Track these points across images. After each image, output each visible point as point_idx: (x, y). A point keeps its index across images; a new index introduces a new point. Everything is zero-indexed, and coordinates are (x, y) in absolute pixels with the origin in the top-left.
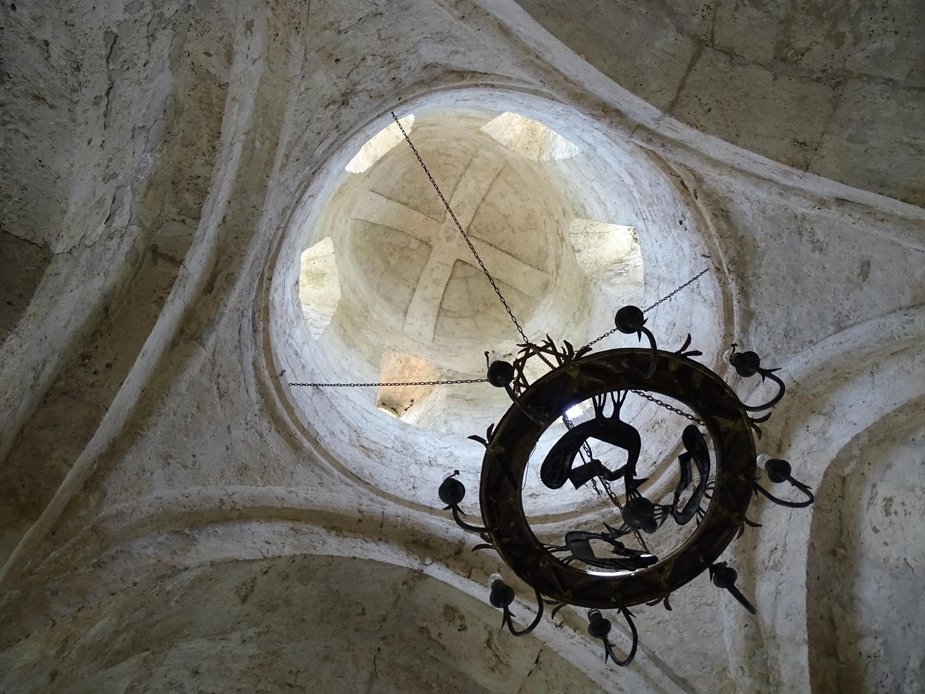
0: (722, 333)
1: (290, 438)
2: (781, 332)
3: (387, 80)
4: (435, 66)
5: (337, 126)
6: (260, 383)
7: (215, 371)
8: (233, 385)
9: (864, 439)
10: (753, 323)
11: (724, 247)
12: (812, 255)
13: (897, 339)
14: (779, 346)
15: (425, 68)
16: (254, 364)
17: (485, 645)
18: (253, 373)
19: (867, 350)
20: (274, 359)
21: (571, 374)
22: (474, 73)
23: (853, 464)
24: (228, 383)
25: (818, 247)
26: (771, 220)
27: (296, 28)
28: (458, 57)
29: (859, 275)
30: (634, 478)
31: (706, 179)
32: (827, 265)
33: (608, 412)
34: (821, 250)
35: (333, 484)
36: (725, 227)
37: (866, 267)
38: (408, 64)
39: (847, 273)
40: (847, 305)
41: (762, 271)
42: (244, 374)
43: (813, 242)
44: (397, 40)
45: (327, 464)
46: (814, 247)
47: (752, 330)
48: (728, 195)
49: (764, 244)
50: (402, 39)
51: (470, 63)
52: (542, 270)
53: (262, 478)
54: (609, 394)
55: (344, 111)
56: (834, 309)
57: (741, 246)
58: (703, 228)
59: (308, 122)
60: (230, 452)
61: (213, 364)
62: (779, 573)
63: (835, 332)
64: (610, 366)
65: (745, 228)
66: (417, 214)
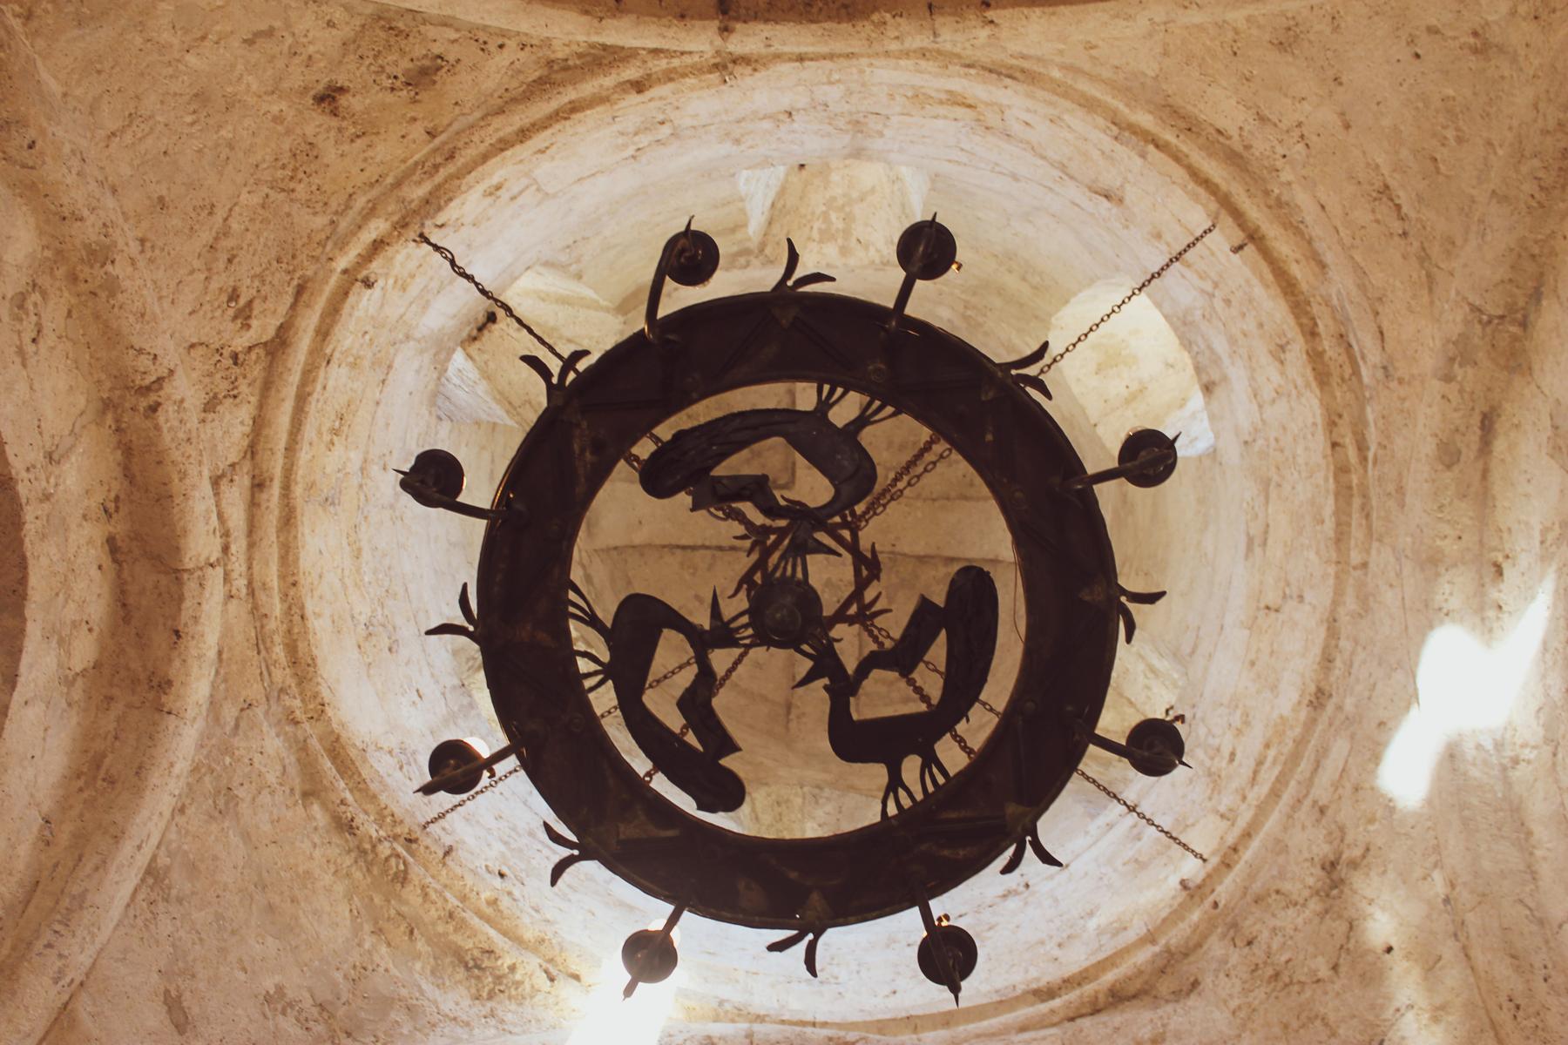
0: (330, 712)
1: (1190, 127)
2: (241, 792)
4: (1179, 995)
5: (1322, 811)
6: (1295, 228)
7: (1416, 244)
8: (1362, 215)
12: (277, 978)
13: (57, 927)
14: (228, 760)
15: (1195, 984)
16: (1323, 266)
18: (1320, 246)
20: (1270, 277)
21: (1021, 809)
22: (1096, 1011)
24: (1377, 221)
26: (387, 1002)
27: (1518, 1007)
29: (180, 997)
30: (826, 681)
32: (241, 976)
33: (911, 767)
34: (268, 999)
35: (1061, 52)
36: (458, 939)
38: (1238, 982)
39: (202, 986)
40: (165, 926)
41: (340, 888)
42: (1340, 241)
43: (290, 1005)
44: (1286, 1026)
45: (1083, 86)
46: (284, 995)
47: (291, 759)
48: (489, 1004)
49: (367, 946)
50: (1277, 1030)
51: (1117, 1029)
52: (608, 550)
53: (1236, 32)
54: (919, 796)
55: (1324, 850)
56: (180, 901)
60: (1331, 73)
61: (1424, 258)
62: (9, 296)
63: (154, 858)
64: (946, 853)
66: (920, 549)
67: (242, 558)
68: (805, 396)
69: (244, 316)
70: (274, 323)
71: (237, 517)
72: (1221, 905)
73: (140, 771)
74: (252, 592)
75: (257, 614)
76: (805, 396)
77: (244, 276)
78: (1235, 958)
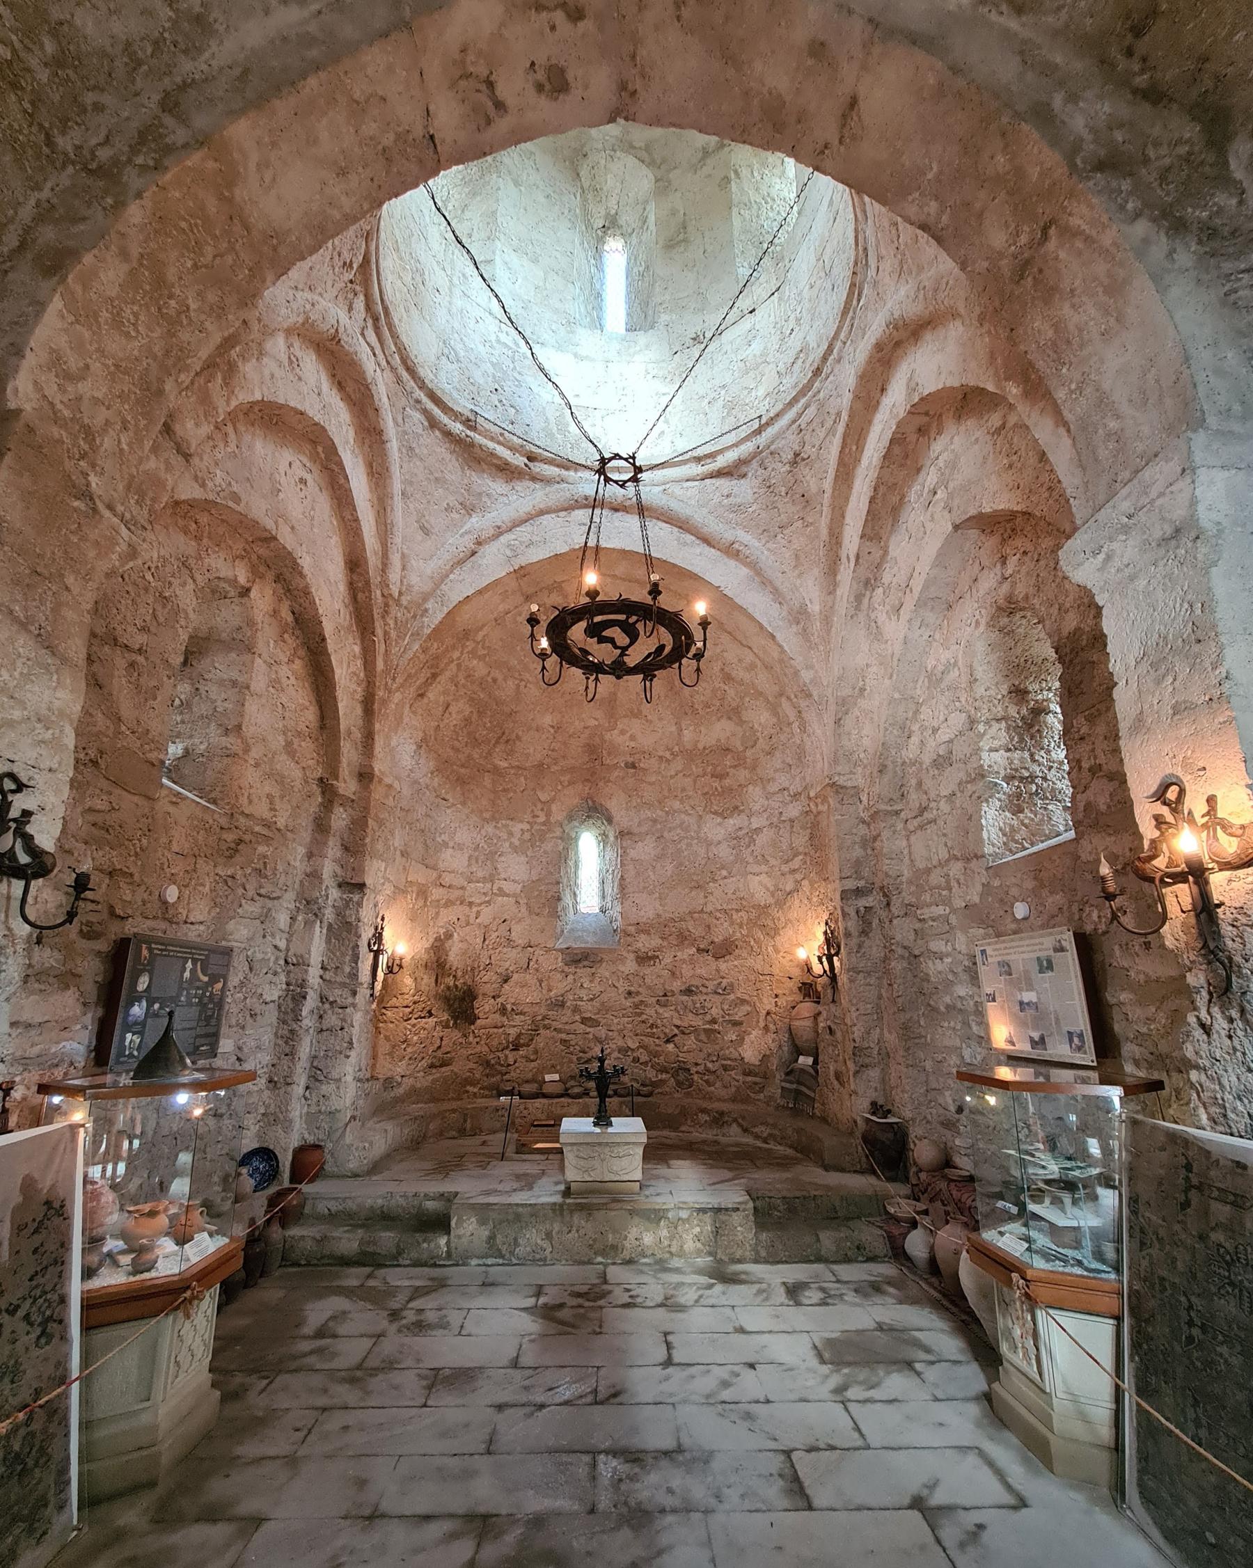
9: (342, 481)
10: (426, 424)
17: (492, 78)
23: (323, 456)
25: (449, 509)
26: (480, 494)
37: (426, 531)
47: (422, 418)
65: (483, 471)
69: (351, 265)
70: (361, 258)
74: (388, 362)
75: (393, 370)
77: (347, 256)
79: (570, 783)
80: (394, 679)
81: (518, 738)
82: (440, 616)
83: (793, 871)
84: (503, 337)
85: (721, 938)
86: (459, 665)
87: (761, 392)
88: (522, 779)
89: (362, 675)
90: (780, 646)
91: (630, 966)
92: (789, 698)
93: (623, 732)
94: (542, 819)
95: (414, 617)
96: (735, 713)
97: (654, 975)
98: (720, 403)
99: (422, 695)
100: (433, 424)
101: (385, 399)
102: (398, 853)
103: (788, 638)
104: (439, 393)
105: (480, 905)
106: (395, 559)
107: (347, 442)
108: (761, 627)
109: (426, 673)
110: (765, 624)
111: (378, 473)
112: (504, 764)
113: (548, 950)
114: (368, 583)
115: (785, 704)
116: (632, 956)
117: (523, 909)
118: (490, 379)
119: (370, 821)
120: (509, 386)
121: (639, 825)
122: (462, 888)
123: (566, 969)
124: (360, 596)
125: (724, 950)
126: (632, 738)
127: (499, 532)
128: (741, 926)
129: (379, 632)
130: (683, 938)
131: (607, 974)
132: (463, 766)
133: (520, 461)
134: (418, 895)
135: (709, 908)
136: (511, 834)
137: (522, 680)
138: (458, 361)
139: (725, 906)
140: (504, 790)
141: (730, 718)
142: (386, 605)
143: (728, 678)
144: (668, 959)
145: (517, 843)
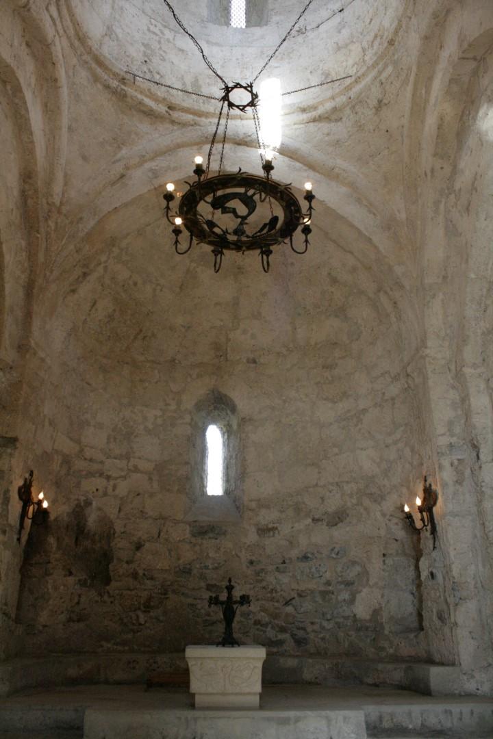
3: (360, 113)
4: (336, 121)
5: (382, 84)
9: (23, 112)
11: (134, 99)
15: (341, 119)
19: (57, 137)
23: (10, 92)
28: (326, 131)
31: (170, 126)
37: (85, 158)
44: (359, 141)
55: (380, 96)
57: (128, 106)
58: (148, 94)
59: (398, 95)
67: (60, 24)
68: (242, 190)
71: (55, 14)
72: (352, 98)
73: (58, 108)
74: (65, 31)
75: (68, 38)
76: (242, 190)
78: (351, 116)
79: (199, 376)
80: (52, 271)
81: (154, 335)
82: (92, 223)
83: (395, 443)
84: (152, 28)
85: (334, 508)
86: (106, 268)
87: (351, 62)
88: (156, 371)
89: (26, 265)
90: (376, 247)
91: (252, 537)
92: (386, 292)
93: (245, 332)
94: (173, 407)
95: (71, 223)
96: (341, 312)
97: (272, 544)
98: (320, 72)
99: (73, 291)
100: (96, 79)
101: (61, 57)
102: (47, 420)
103: (382, 241)
104: (102, 58)
105: (116, 478)
106: (60, 176)
107: (29, 85)
108: (360, 232)
109: (78, 272)
110: (362, 228)
111: (51, 110)
112: (142, 358)
113: (176, 522)
114: (36, 191)
115: (383, 299)
116: (254, 529)
117: (155, 485)
118: (141, 54)
119: (24, 386)
120: (156, 60)
121: (260, 412)
122: (102, 462)
123: (193, 540)
124: (30, 202)
125: (337, 518)
126: (253, 336)
127: (143, 160)
128: (351, 496)
129: (42, 230)
130: (298, 509)
131: (230, 545)
132: (105, 357)
133: (162, 109)
134: (62, 463)
135: (321, 483)
136: (145, 418)
137: (158, 285)
138: (117, 40)
139: (336, 480)
140: (141, 381)
141: (336, 316)
142: (50, 211)
143: (334, 281)
144: (285, 529)
145: (151, 427)
